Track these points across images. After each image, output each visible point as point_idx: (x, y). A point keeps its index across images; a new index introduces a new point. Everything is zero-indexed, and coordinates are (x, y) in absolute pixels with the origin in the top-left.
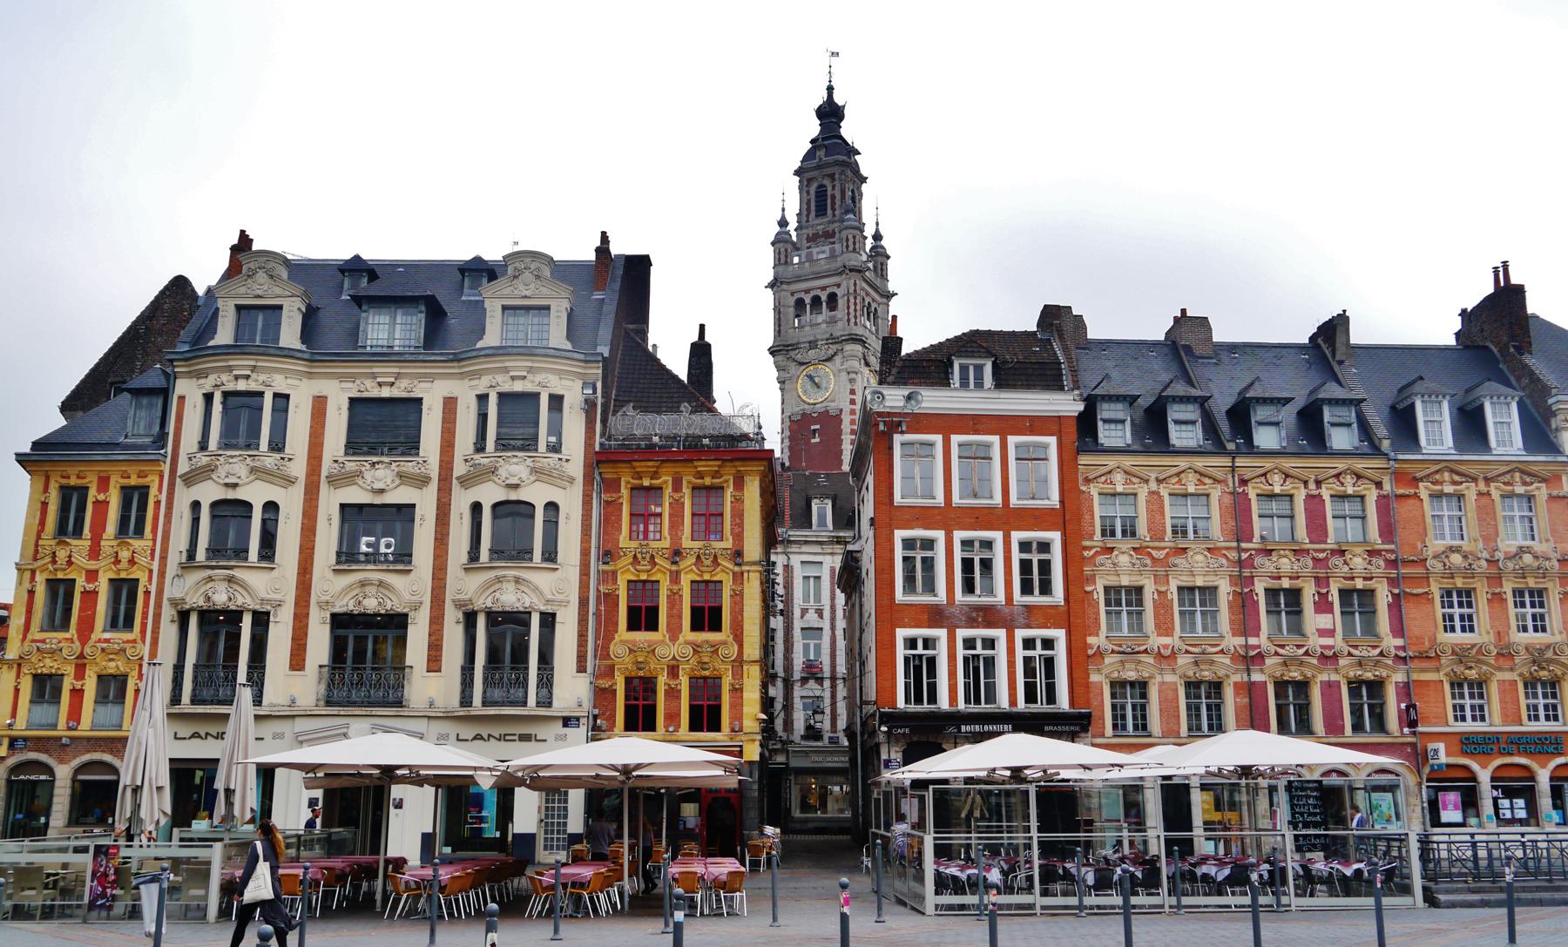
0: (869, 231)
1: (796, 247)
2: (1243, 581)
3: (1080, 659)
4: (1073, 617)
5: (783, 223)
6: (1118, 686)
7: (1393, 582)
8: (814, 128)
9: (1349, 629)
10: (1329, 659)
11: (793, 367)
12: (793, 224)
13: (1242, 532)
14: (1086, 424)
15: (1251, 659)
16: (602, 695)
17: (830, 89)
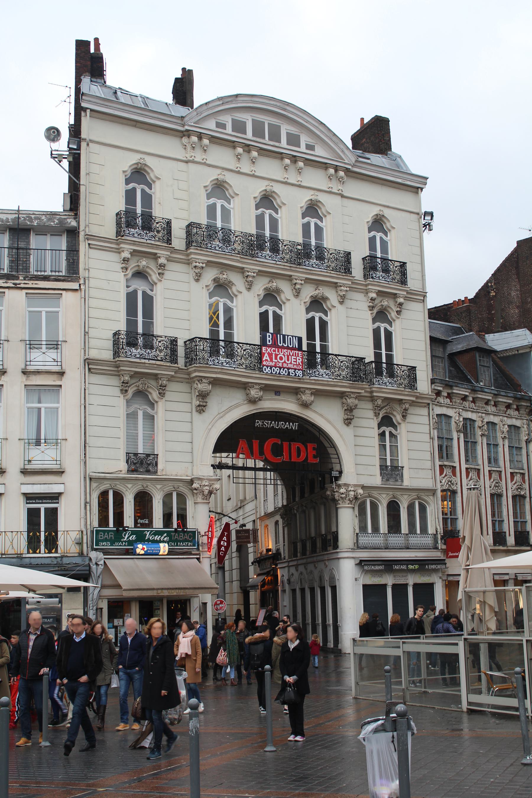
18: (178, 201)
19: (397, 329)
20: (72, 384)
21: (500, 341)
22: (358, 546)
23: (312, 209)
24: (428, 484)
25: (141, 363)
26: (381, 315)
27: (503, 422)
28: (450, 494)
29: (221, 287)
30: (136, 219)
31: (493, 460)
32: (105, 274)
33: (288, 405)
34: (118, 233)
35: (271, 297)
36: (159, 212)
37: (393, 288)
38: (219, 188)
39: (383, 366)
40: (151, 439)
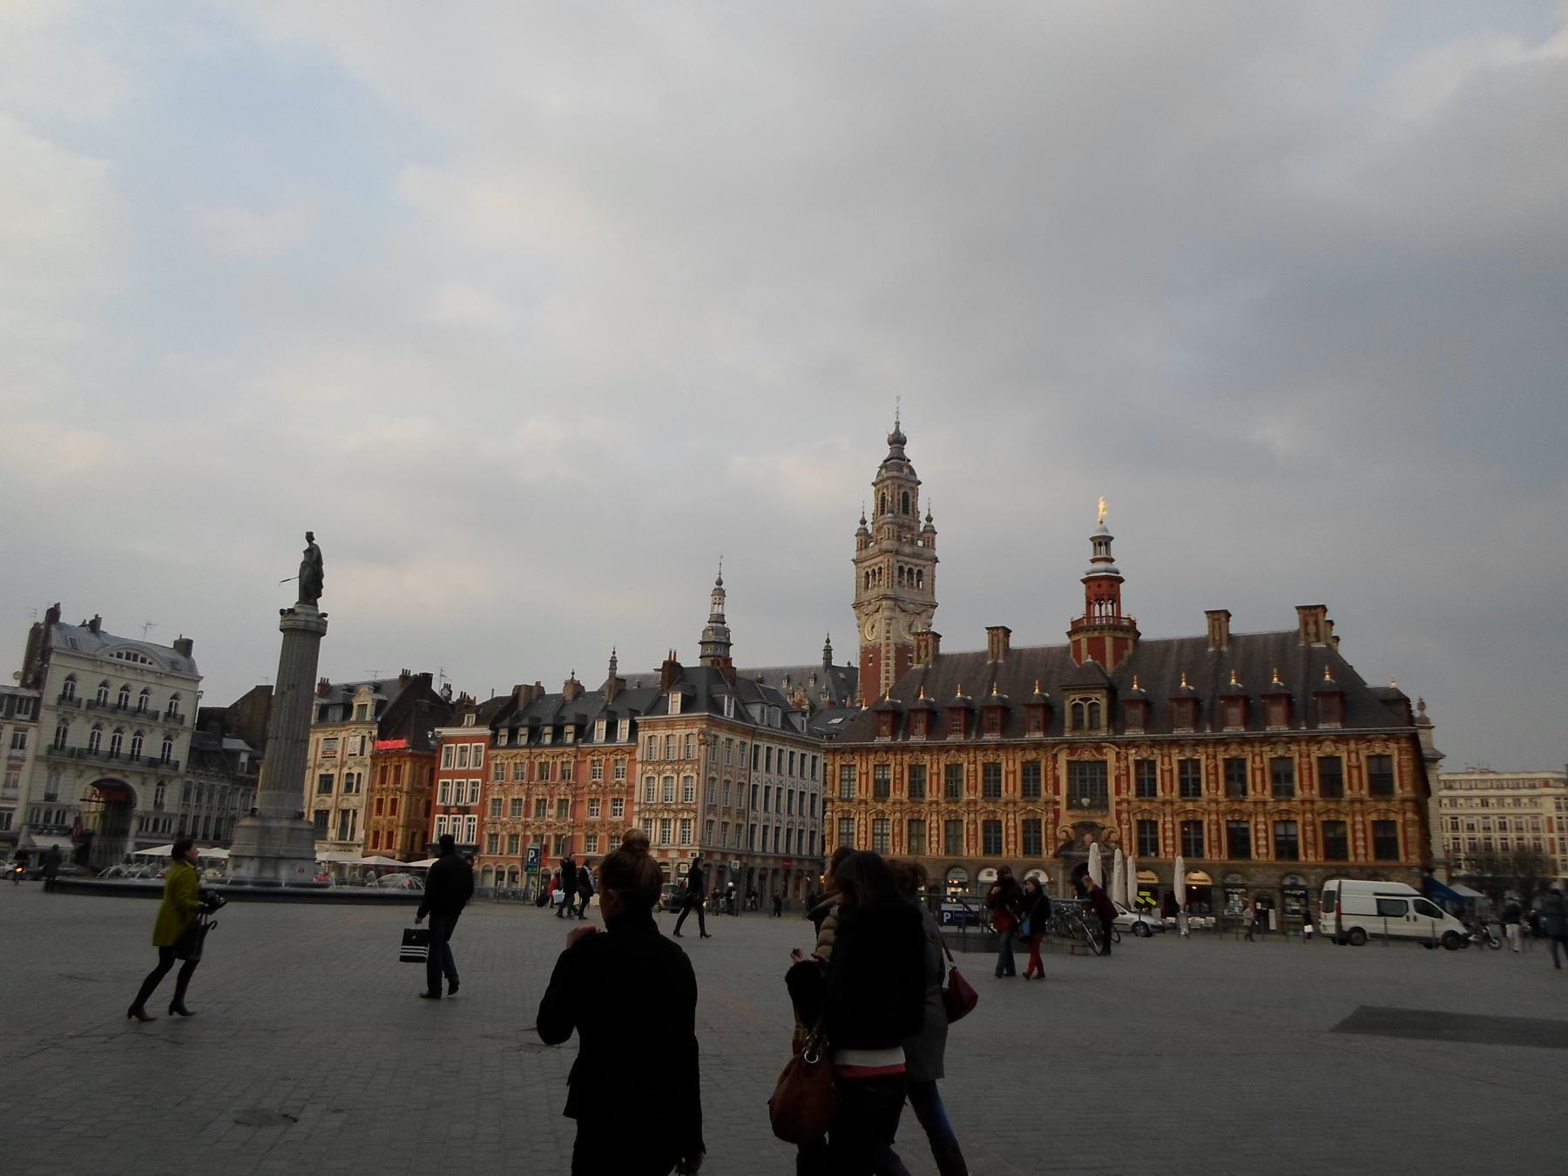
0: (922, 518)
1: (870, 536)
2: (528, 796)
3: (482, 825)
4: (481, 811)
5: (863, 522)
6: (491, 836)
7: (574, 796)
8: (886, 451)
9: (559, 814)
10: (549, 826)
11: (864, 618)
12: (869, 519)
13: (530, 779)
14: (495, 736)
15: (526, 826)
16: (367, 836)
17: (898, 424)
18: (86, 690)
19: (174, 744)
20: (27, 766)
21: (231, 744)
22: (137, 836)
23: (145, 692)
24: (174, 811)
25: (59, 755)
26: (168, 738)
27: (218, 785)
28: (184, 816)
29: (97, 726)
30: (66, 698)
31: (210, 801)
32: (49, 720)
33: (118, 776)
34: (59, 704)
35: (118, 730)
36: (77, 694)
37: (177, 726)
38: (105, 684)
39: (164, 761)
40: (56, 786)
